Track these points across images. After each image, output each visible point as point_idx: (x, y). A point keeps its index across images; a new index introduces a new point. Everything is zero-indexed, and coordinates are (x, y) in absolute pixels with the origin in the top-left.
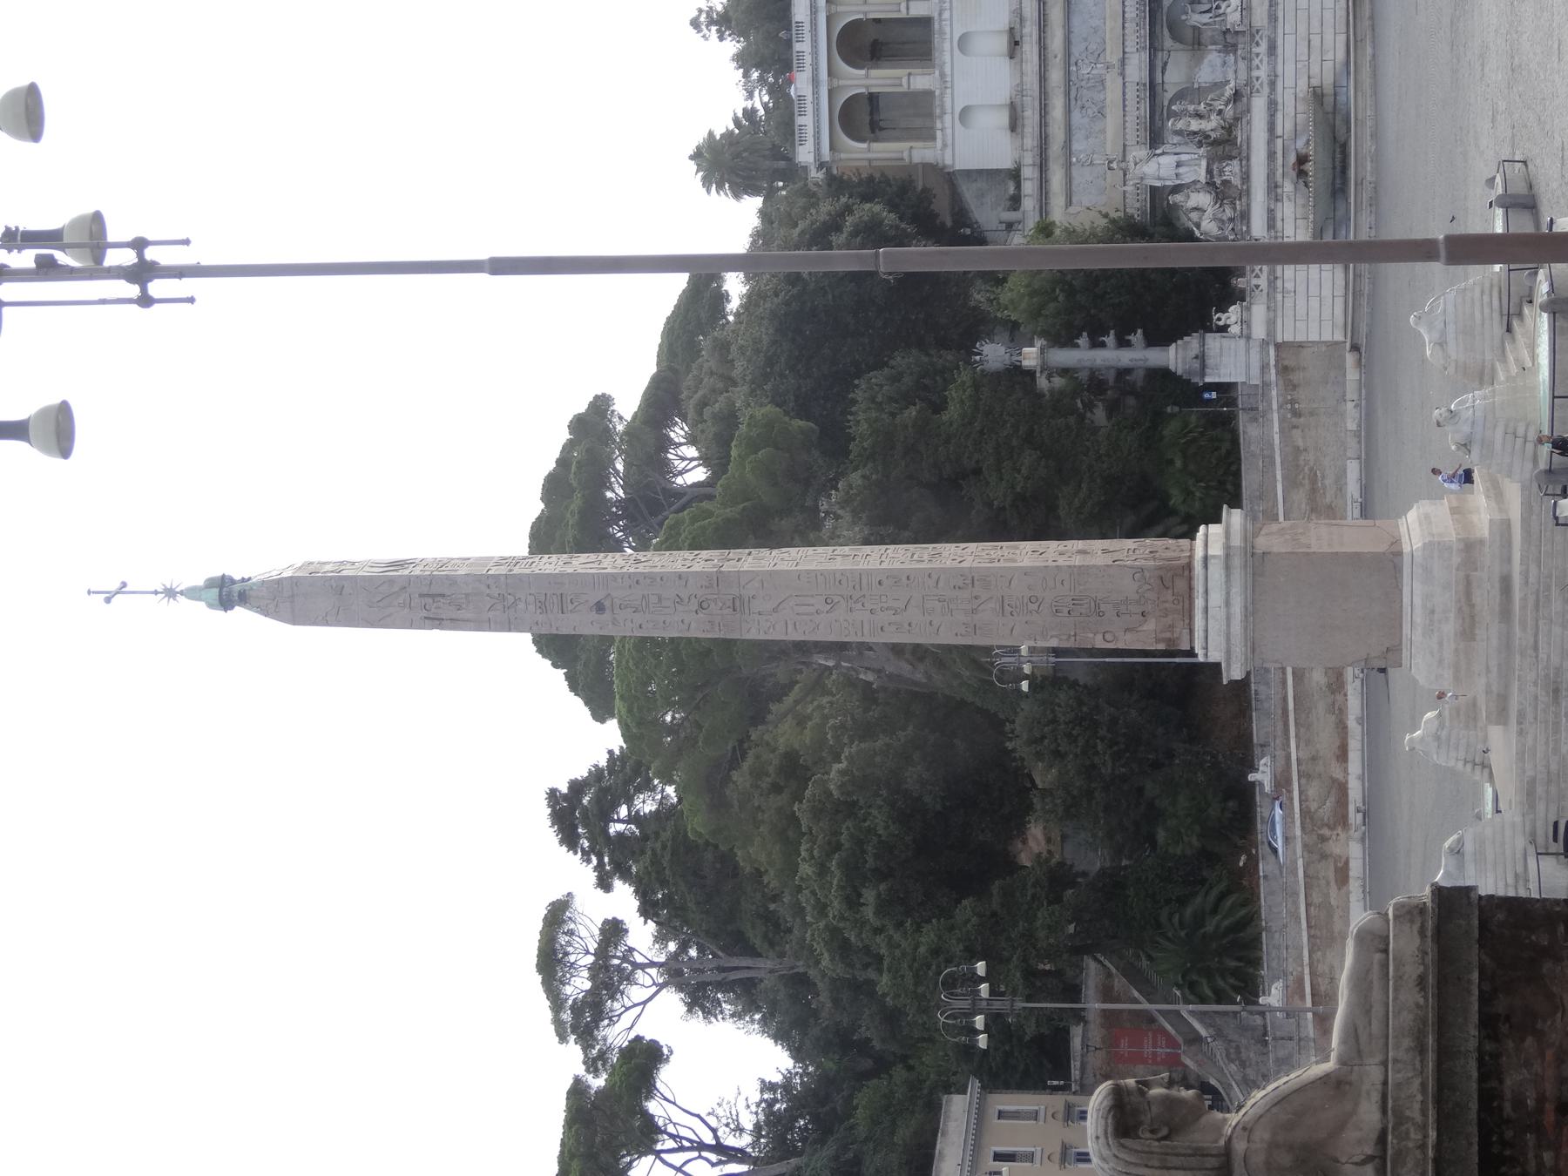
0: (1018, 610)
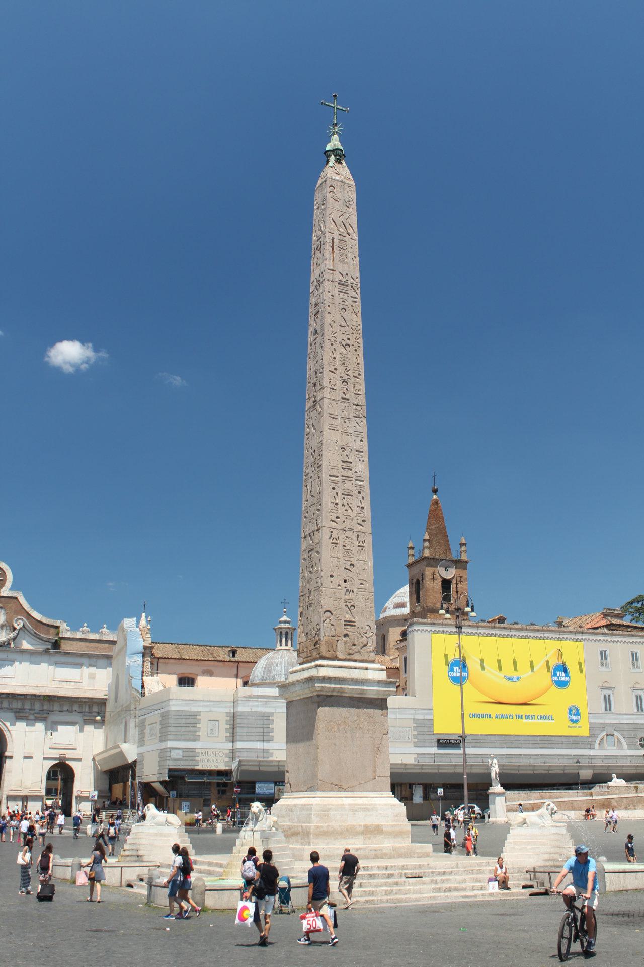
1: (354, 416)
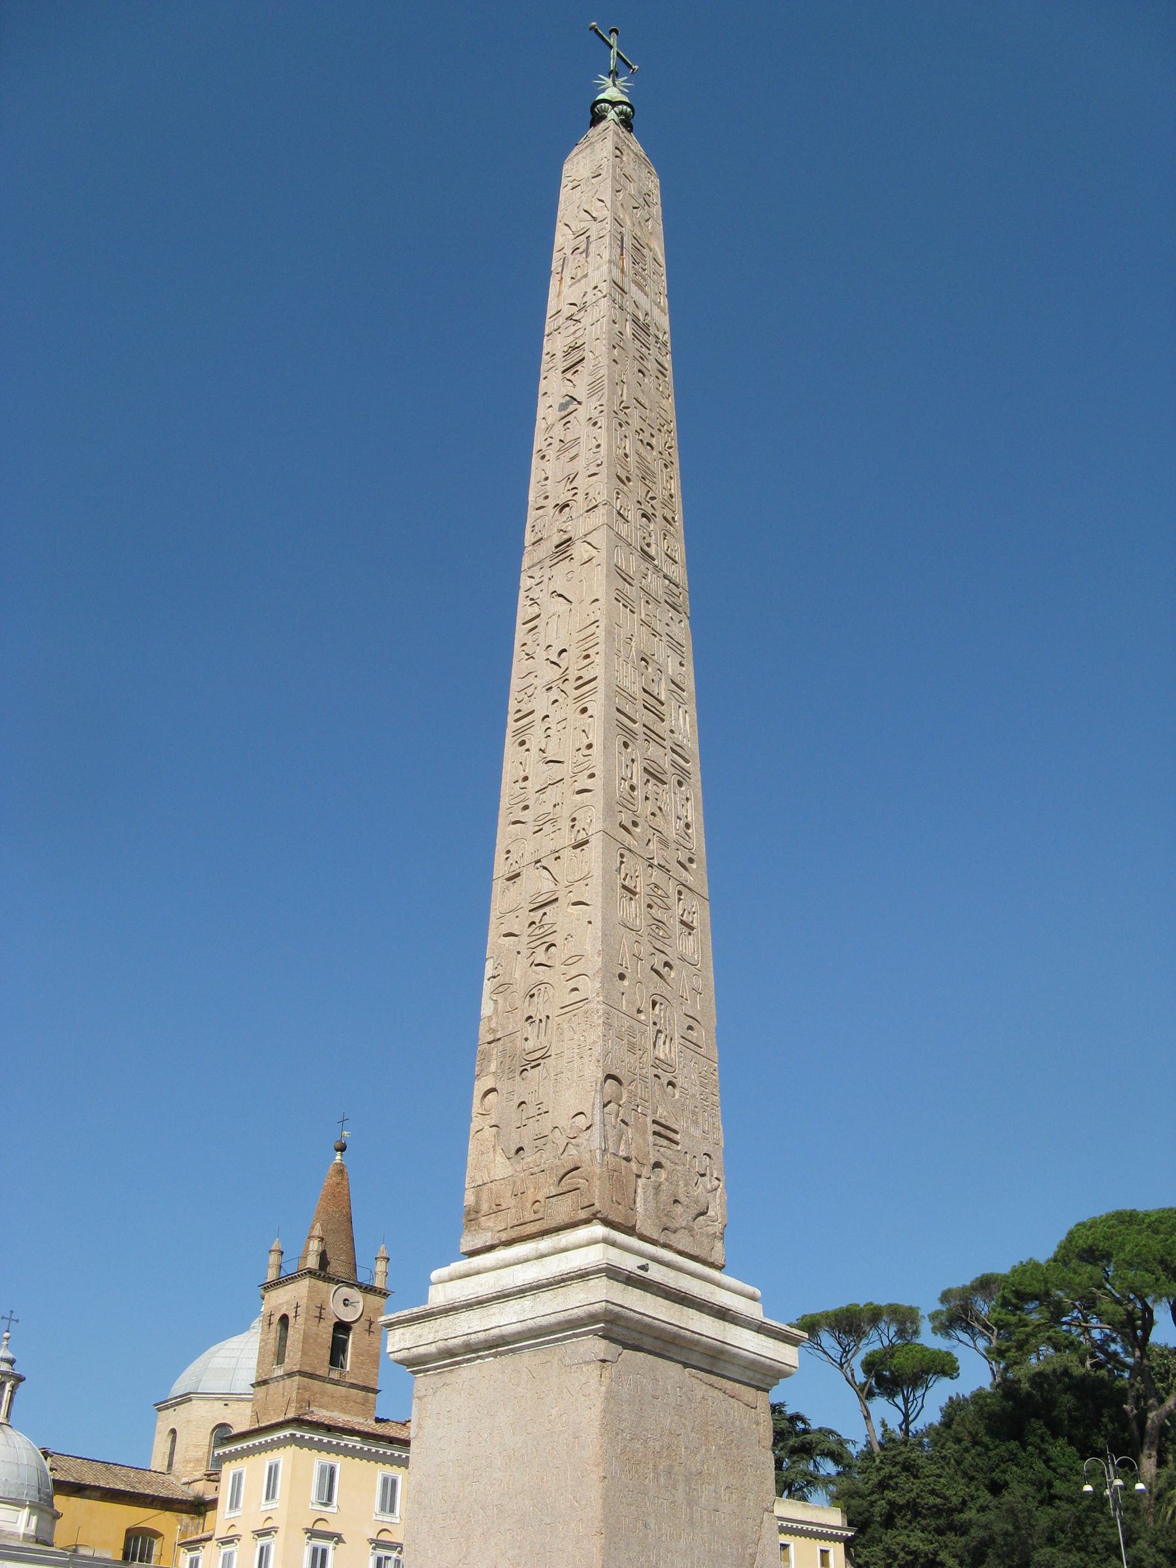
0: (537, 932)
1: (666, 601)
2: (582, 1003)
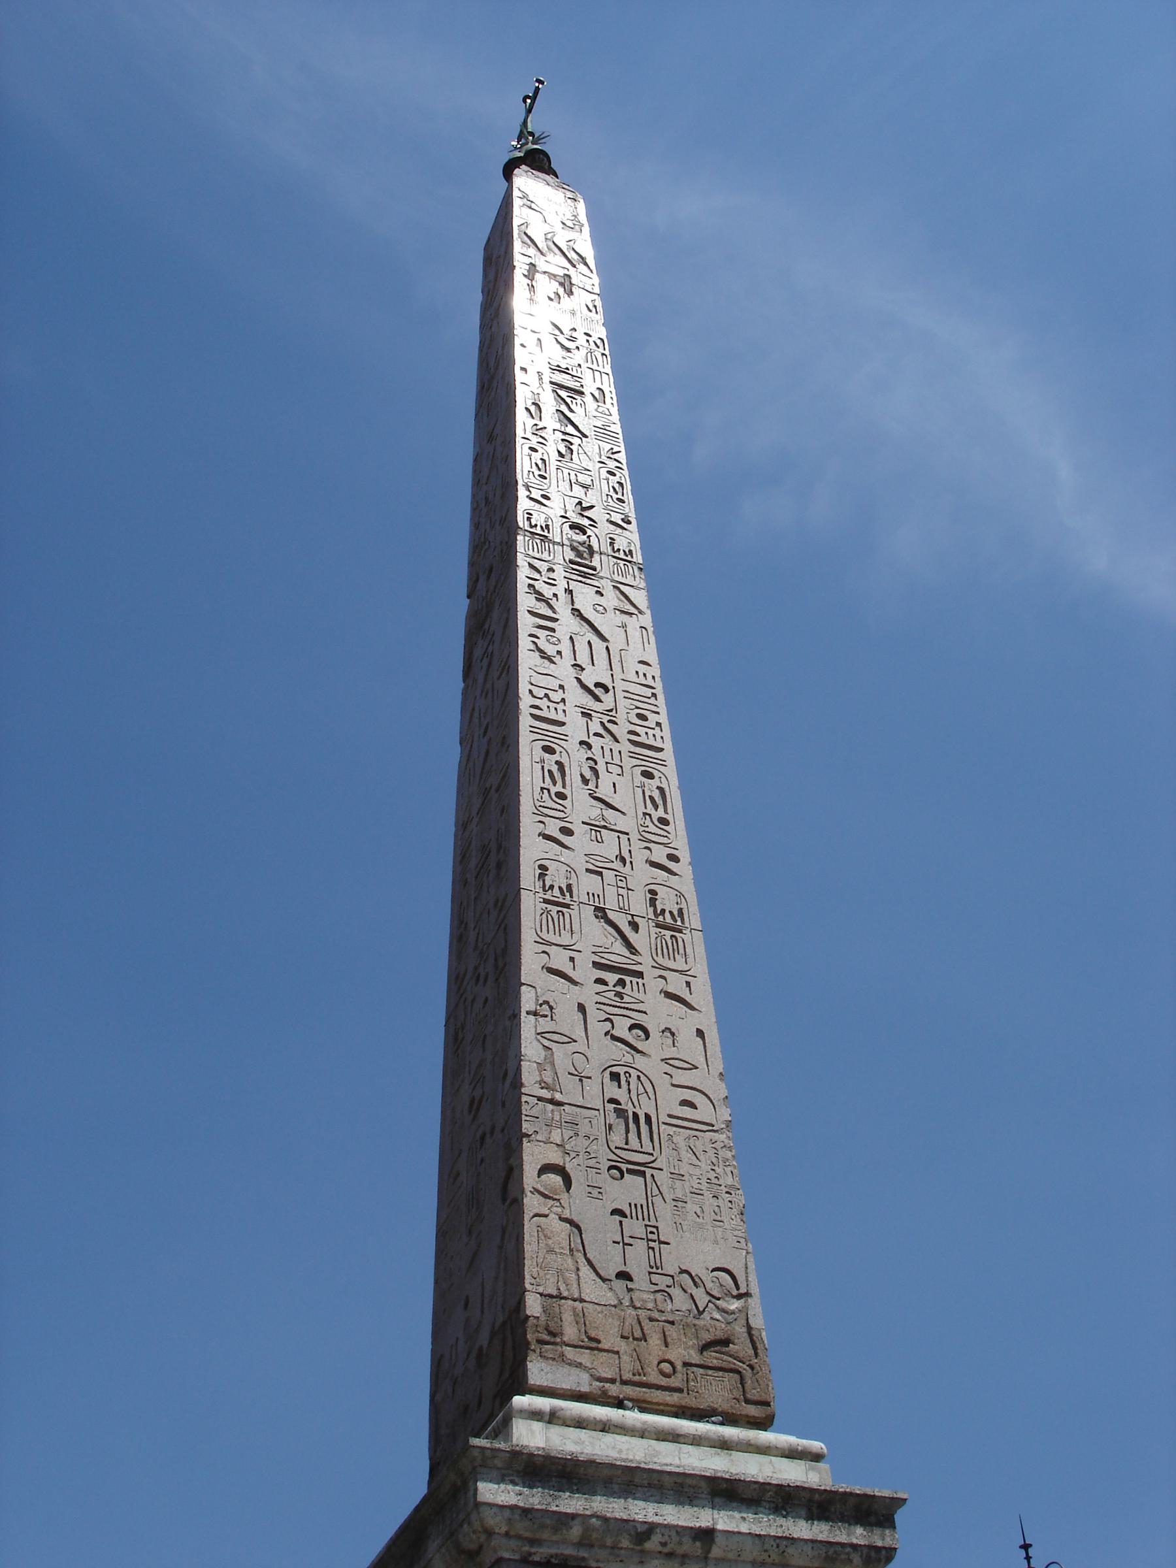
2: (705, 1128)
